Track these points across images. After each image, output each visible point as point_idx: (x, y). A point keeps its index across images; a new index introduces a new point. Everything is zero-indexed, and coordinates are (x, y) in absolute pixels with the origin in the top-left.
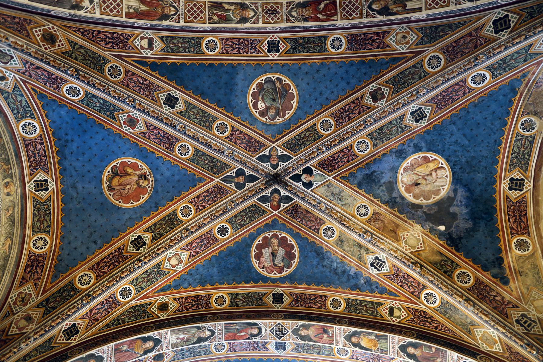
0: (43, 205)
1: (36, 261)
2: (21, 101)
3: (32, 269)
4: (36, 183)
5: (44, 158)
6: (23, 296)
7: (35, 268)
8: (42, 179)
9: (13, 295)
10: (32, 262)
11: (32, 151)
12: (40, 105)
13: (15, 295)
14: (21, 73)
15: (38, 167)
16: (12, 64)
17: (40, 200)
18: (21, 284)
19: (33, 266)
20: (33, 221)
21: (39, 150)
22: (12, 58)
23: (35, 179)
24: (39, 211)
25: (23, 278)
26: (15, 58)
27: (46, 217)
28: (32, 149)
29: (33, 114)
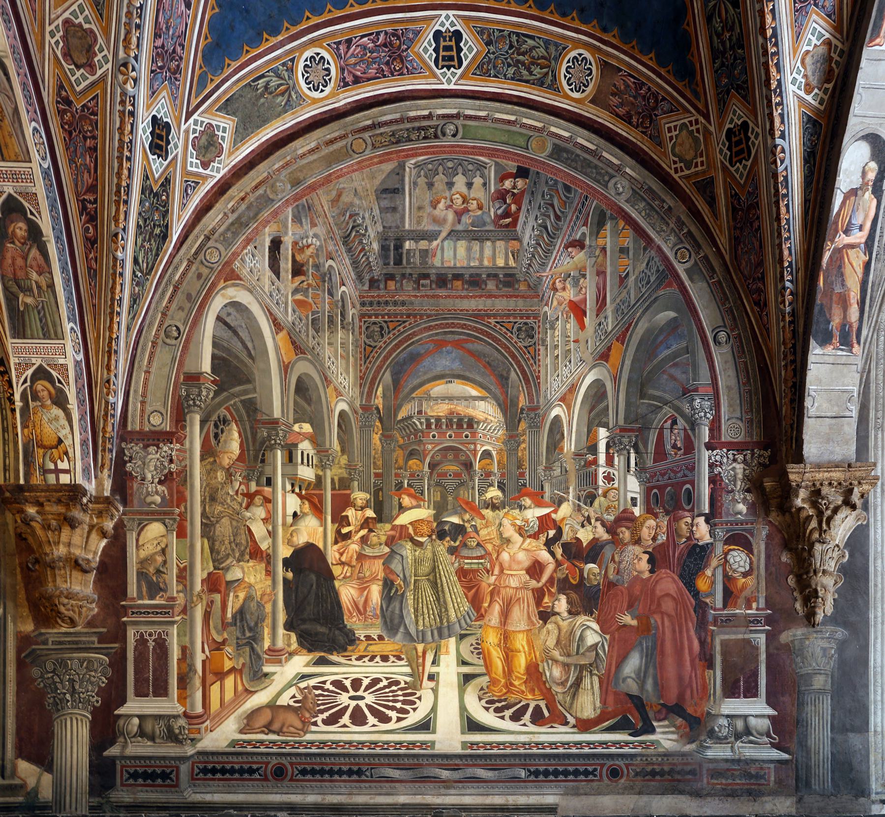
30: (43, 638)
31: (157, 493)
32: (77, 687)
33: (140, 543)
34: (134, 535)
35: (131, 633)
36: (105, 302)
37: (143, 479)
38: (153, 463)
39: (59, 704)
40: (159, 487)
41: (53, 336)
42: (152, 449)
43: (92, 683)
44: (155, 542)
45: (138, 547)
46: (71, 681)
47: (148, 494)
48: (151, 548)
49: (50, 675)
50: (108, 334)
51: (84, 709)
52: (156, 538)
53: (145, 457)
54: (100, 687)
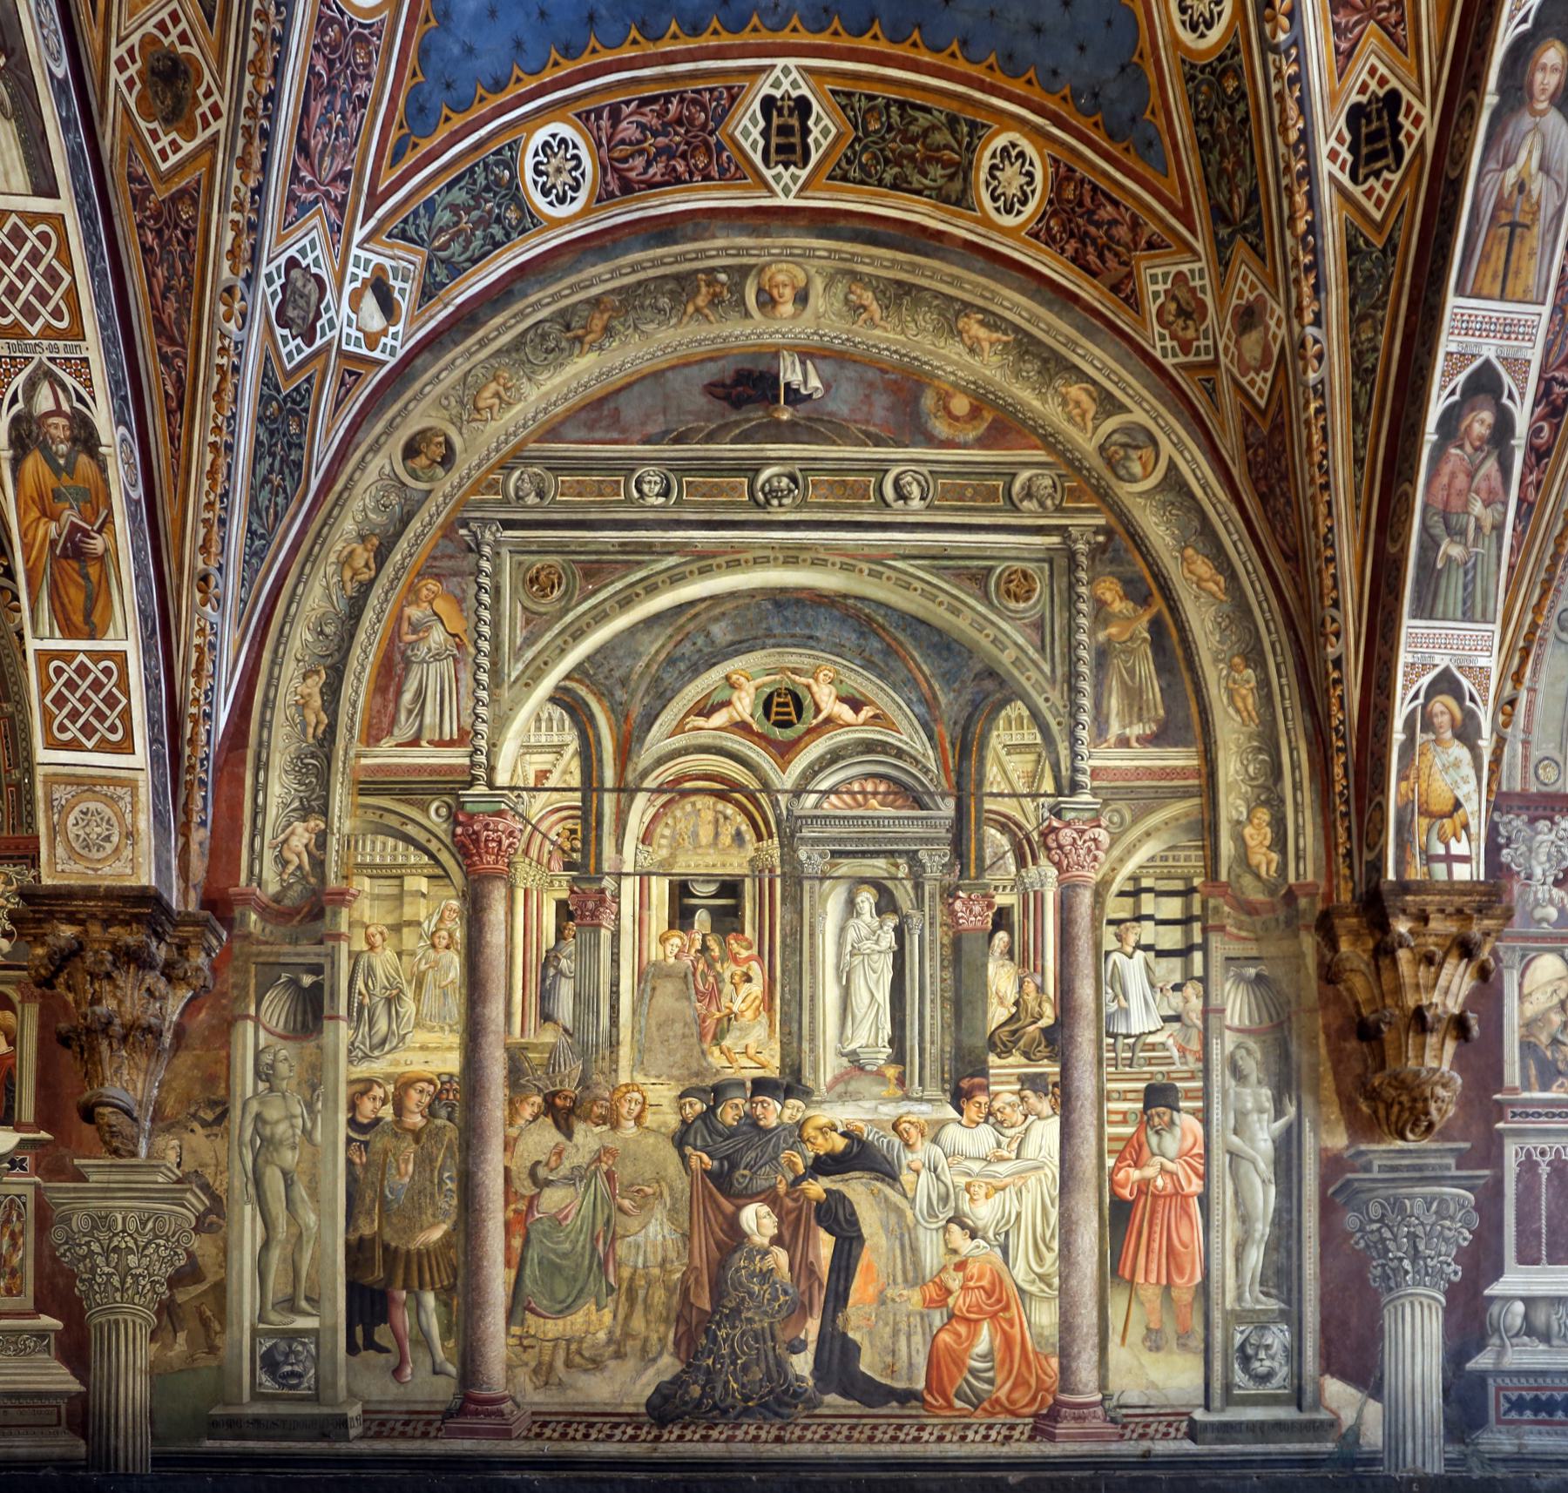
0: (867, 134)
1: (1075, 217)
2: (454, 208)
3: (1094, 241)
4: (773, 157)
5: (673, 107)
6: (1173, 307)
7: (1092, 230)
8: (762, 124)
9: (1159, 344)
10: (1072, 235)
11: (649, 164)
12: (458, 121)
13: (1162, 338)
14: (342, 216)
15: (713, 140)
16: (316, 260)
17: (843, 148)
18: (1133, 302)
19: (1086, 233)
20: (919, 193)
21: (642, 126)
22: (292, 263)
23: (757, 158)
24: (887, 161)
25: (1115, 289)
26: (292, 252)
27: (914, 129)
28: (639, 162)
29: (498, 152)
30: (1363, 1160)
31: (1551, 901)
32: (1421, 1247)
33: (1526, 990)
34: (1516, 974)
35: (1511, 1150)
36: (1539, 560)
37: (1529, 877)
38: (1544, 850)
39: (1393, 1277)
40: (1555, 891)
41: (1478, 615)
42: (1543, 825)
43: (1446, 1240)
44: (1550, 990)
45: (1521, 997)
46: (1413, 1237)
47: (1537, 904)
48: (1543, 998)
49: (1375, 1226)
50: (1529, 618)
51: (1434, 1286)
52: (1550, 982)
53: (1532, 839)
54: (1459, 1247)
